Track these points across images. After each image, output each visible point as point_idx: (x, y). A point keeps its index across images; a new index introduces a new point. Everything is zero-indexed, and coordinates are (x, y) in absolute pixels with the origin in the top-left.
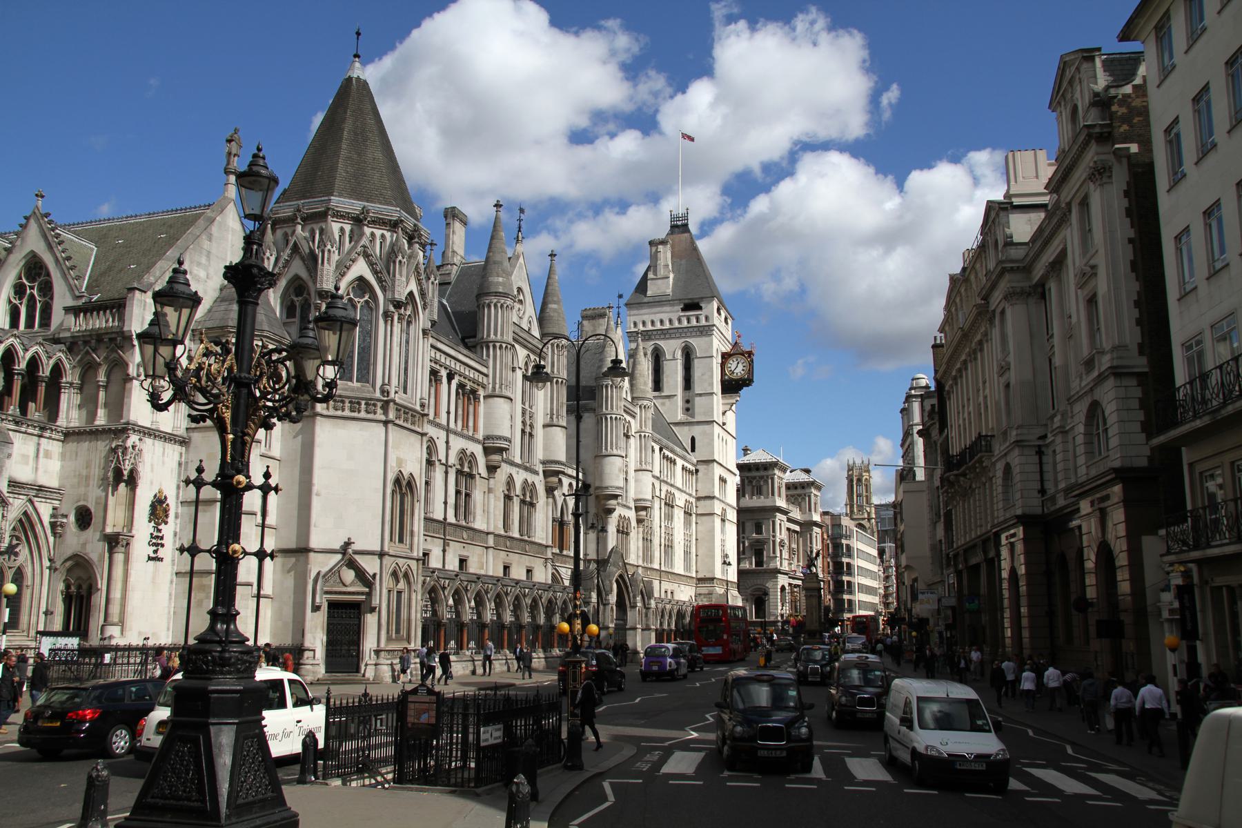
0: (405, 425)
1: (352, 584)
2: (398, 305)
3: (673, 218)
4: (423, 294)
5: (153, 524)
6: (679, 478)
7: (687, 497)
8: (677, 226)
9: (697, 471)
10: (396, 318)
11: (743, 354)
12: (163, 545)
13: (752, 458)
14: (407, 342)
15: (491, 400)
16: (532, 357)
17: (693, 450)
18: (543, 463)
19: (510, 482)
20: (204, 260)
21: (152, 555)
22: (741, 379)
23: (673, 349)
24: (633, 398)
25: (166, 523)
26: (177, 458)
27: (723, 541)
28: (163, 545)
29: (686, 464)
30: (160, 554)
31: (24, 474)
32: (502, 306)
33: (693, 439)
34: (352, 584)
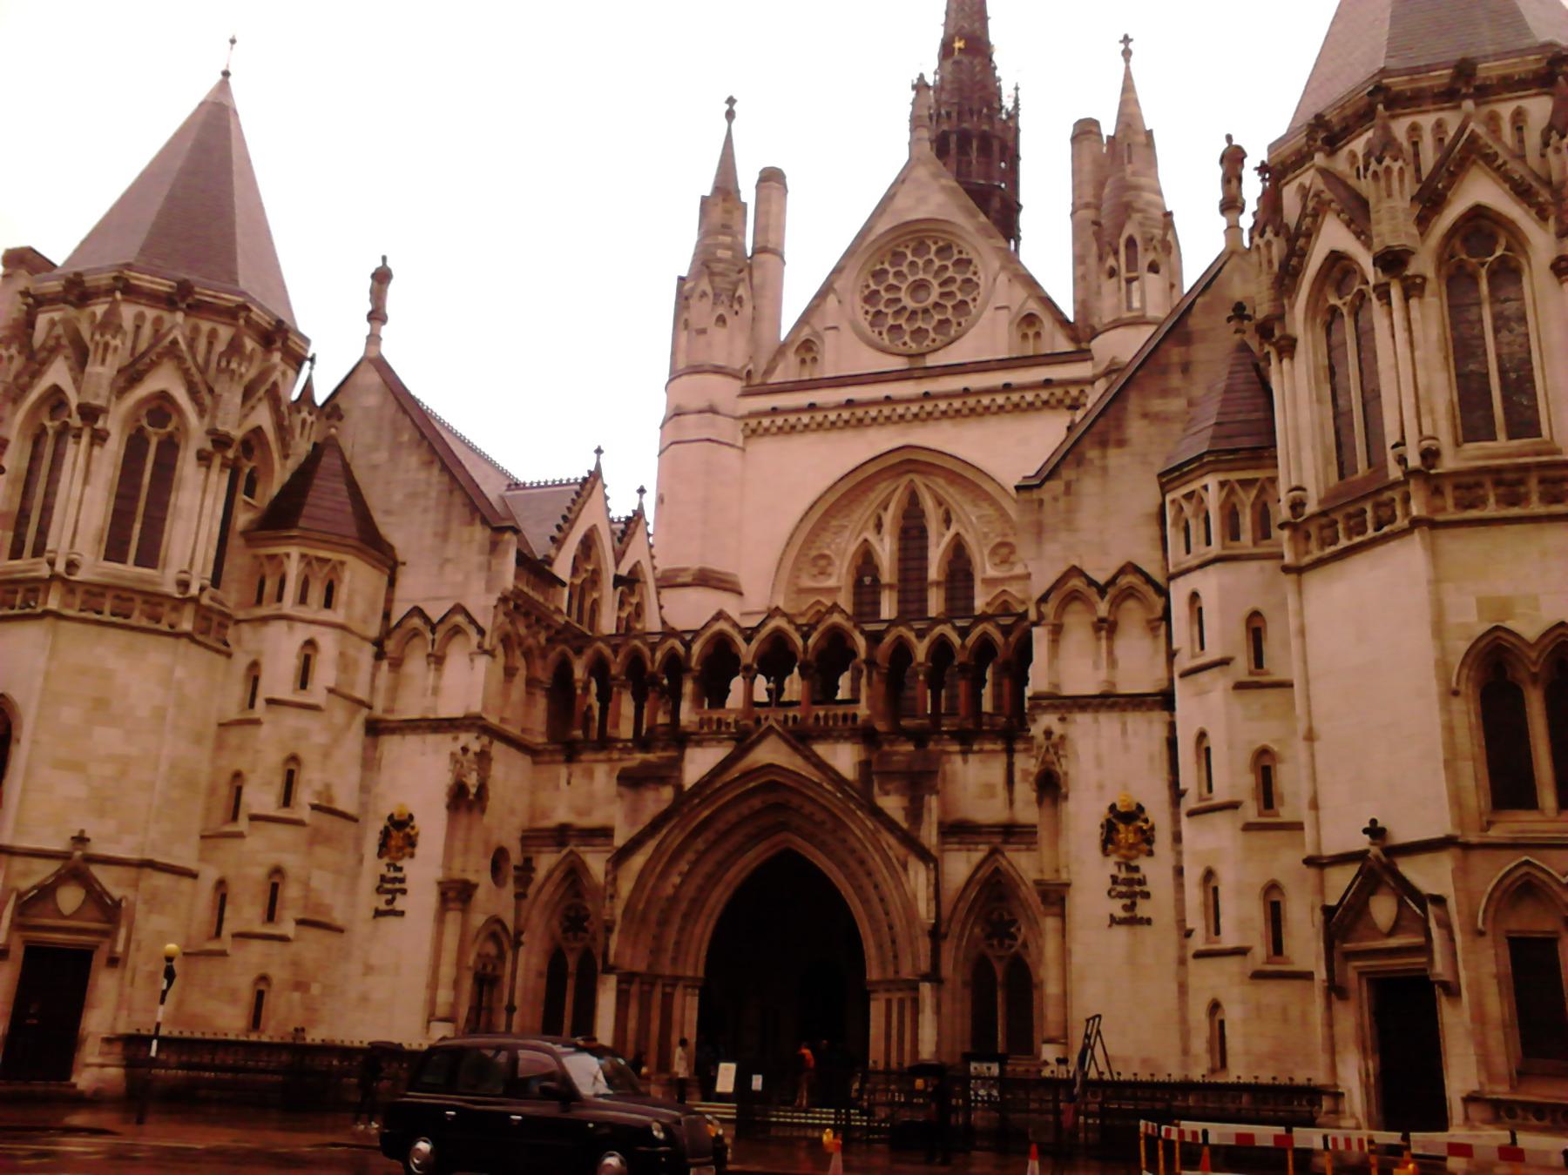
0: (1515, 511)
1: (1393, 931)
2: (1392, 261)
4: (1522, 192)
5: (1114, 858)
10: (1396, 293)
12: (1147, 895)
14: (1512, 321)
20: (1175, 380)
21: (1120, 914)
25: (1150, 853)
26: (1160, 732)
28: (1147, 895)
30: (1143, 909)
31: (991, 811)
34: (1393, 931)
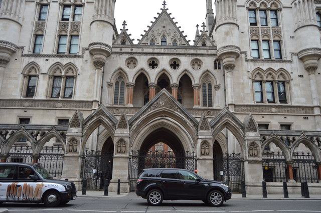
19: (33, 66)
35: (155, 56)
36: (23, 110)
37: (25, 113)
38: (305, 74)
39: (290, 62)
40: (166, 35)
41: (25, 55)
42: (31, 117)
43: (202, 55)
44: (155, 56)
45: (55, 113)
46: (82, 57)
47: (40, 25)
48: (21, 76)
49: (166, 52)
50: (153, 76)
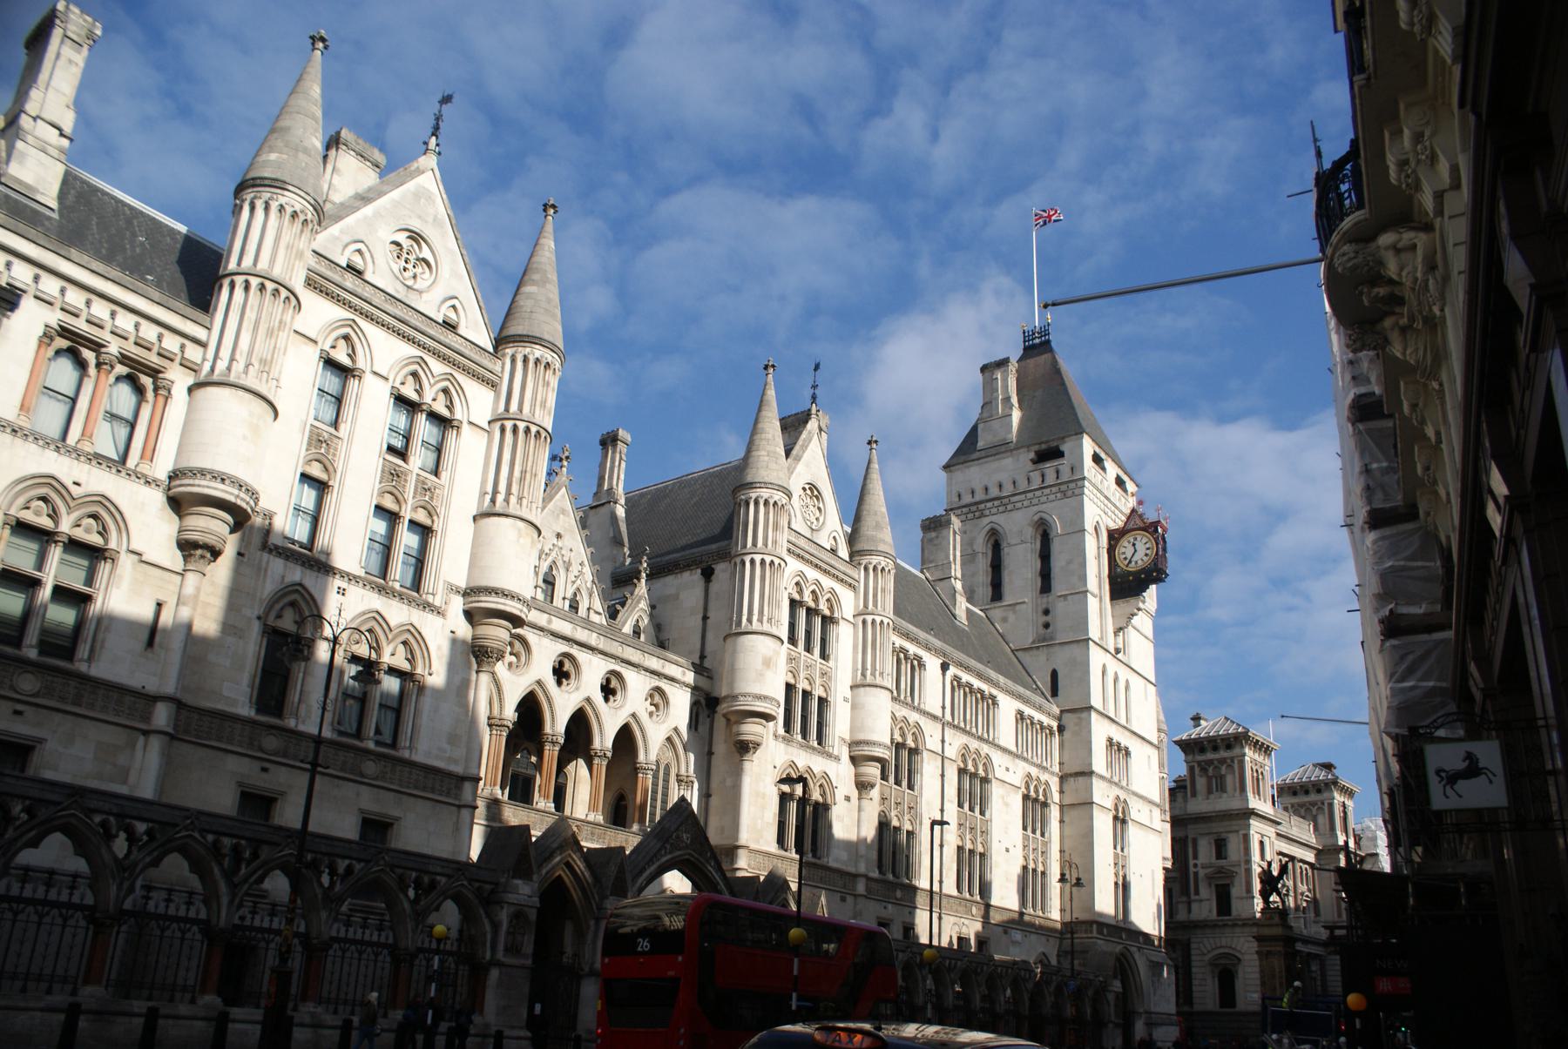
3: (1027, 336)
6: (1006, 730)
7: (1034, 771)
8: (1034, 347)
9: (1061, 729)
11: (1144, 529)
13: (1206, 728)
15: (202, 393)
16: (437, 367)
17: (1055, 693)
18: (468, 593)
22: (1143, 571)
23: (1017, 526)
24: (851, 555)
27: (1120, 863)
29: (1028, 711)
32: (875, 568)
33: (1054, 674)
35: (574, 651)
36: (257, 765)
37: (264, 775)
38: (854, 793)
39: (837, 759)
40: (560, 563)
41: (277, 547)
42: (283, 794)
43: (672, 679)
44: (574, 651)
45: (358, 794)
46: (438, 612)
47: (321, 443)
48: (256, 627)
49: (601, 646)
50: (560, 709)
